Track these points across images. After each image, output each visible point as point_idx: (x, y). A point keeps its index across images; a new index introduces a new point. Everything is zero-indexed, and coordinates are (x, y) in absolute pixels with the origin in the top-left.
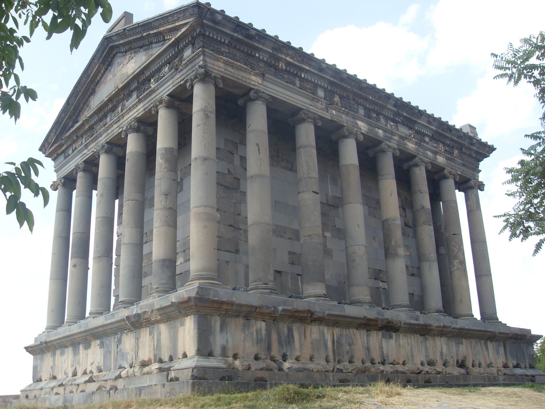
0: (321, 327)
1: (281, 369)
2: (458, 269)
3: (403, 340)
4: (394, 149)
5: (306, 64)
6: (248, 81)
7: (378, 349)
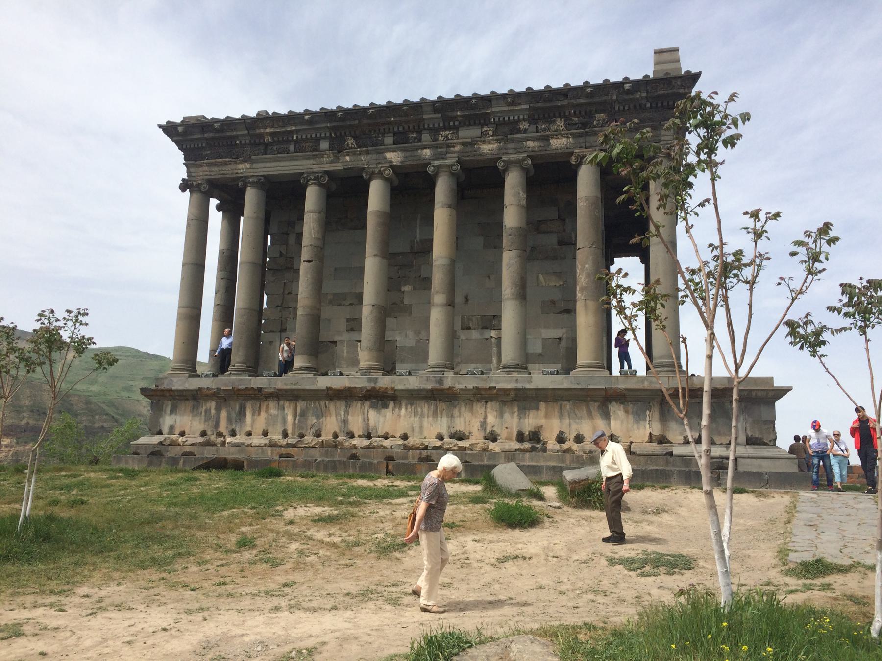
1: (223, 444)
3: (406, 409)
4: (449, 166)
5: (291, 125)
6: (235, 172)
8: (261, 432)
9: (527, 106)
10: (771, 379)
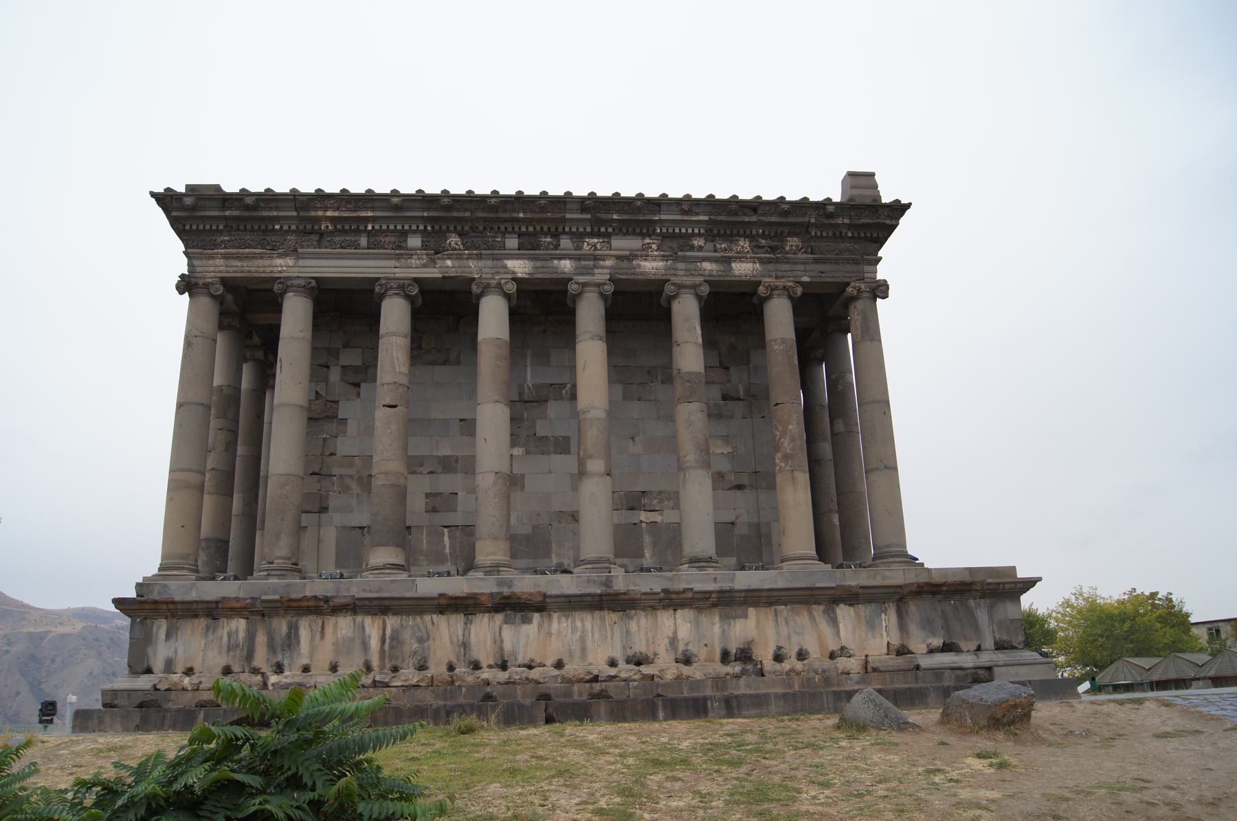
0: (359, 618)
2: (781, 470)
4: (598, 285)
5: (367, 209)
6: (268, 270)
7: (489, 642)
8: (327, 666)
9: (706, 218)
10: (1014, 568)
